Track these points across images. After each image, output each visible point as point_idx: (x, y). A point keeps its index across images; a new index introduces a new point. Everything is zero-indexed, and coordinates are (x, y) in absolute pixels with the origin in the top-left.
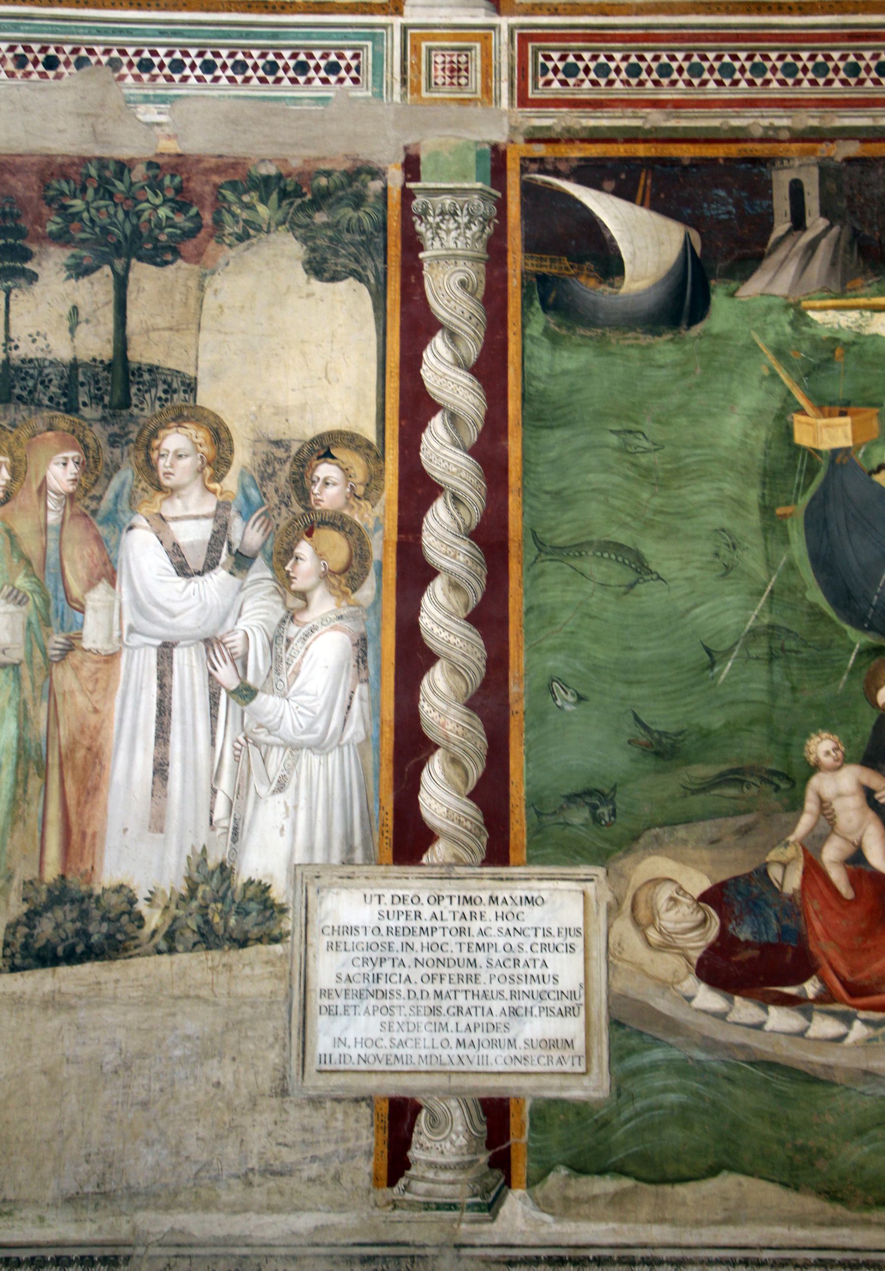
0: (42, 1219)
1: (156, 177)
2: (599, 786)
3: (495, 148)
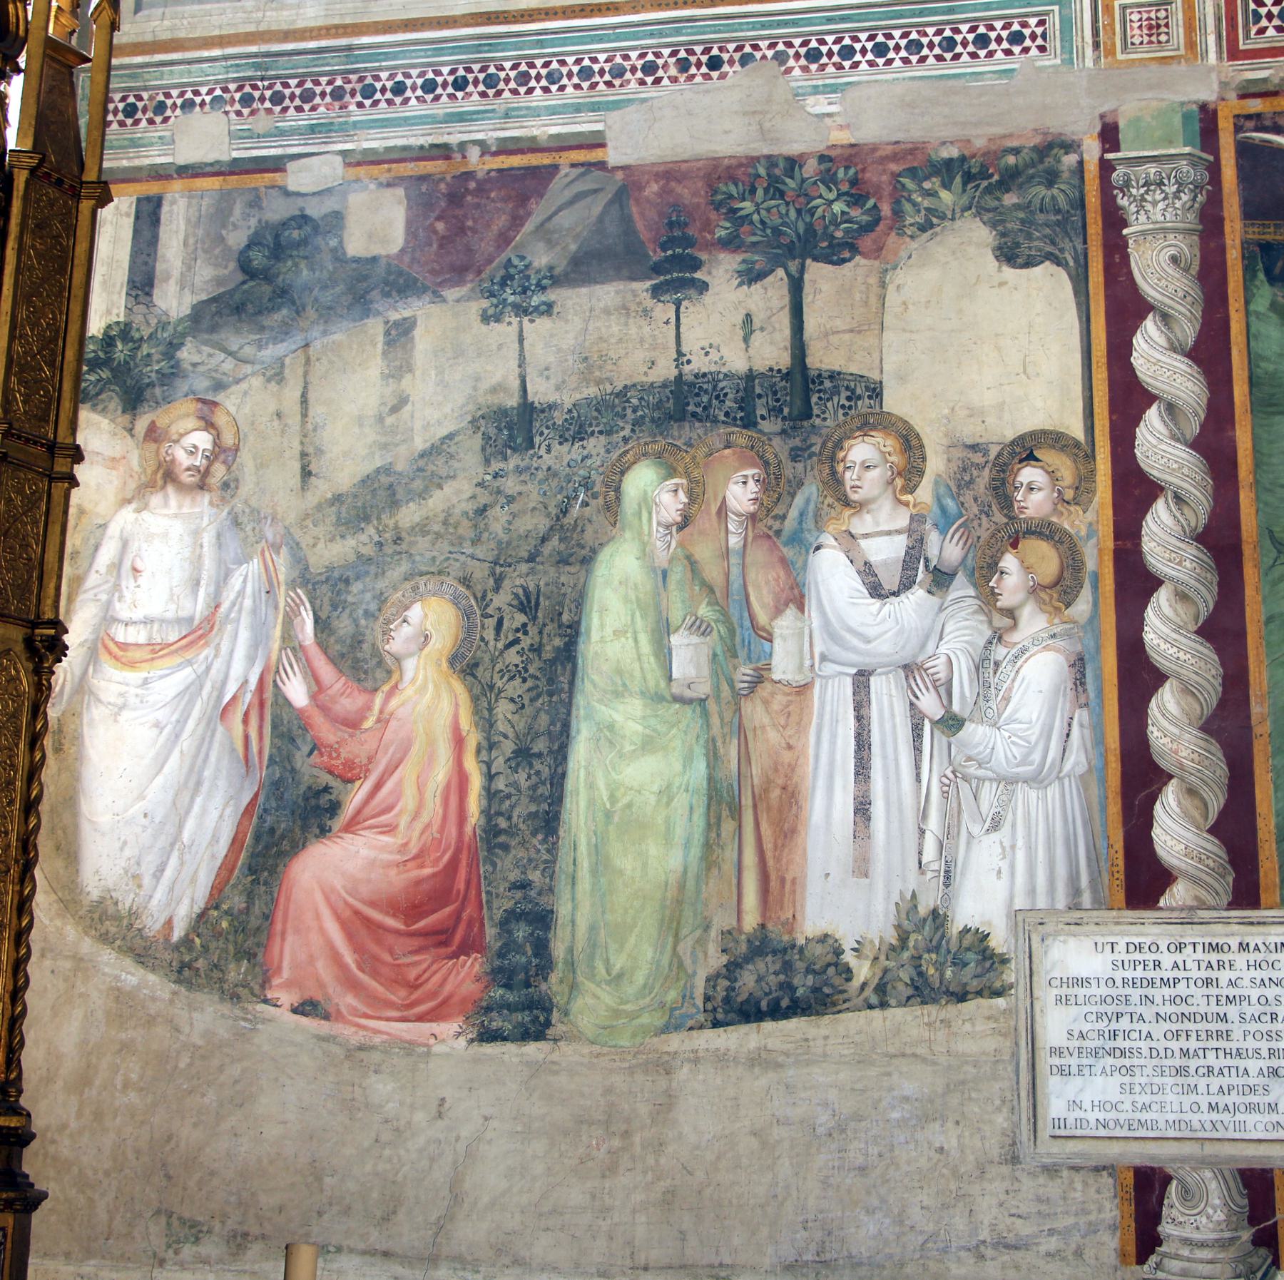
1: (829, 170)
3: (1203, 107)
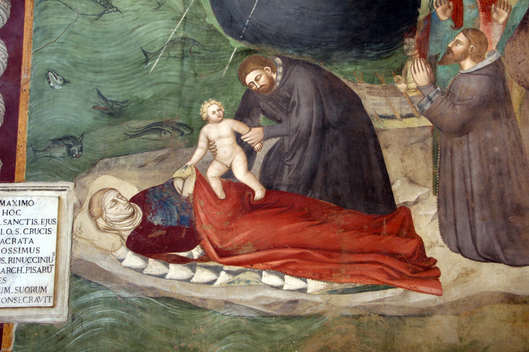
2: (73, 134)
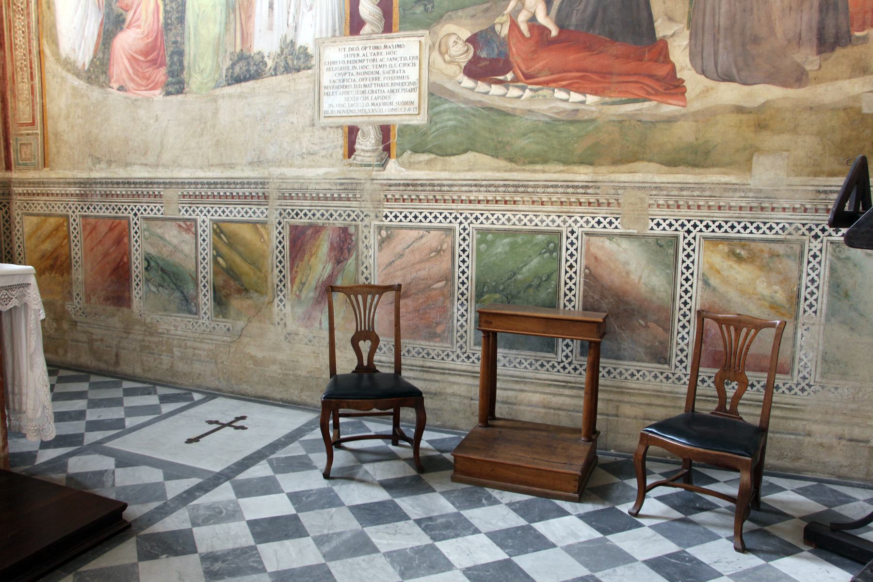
0: (243, 170)
